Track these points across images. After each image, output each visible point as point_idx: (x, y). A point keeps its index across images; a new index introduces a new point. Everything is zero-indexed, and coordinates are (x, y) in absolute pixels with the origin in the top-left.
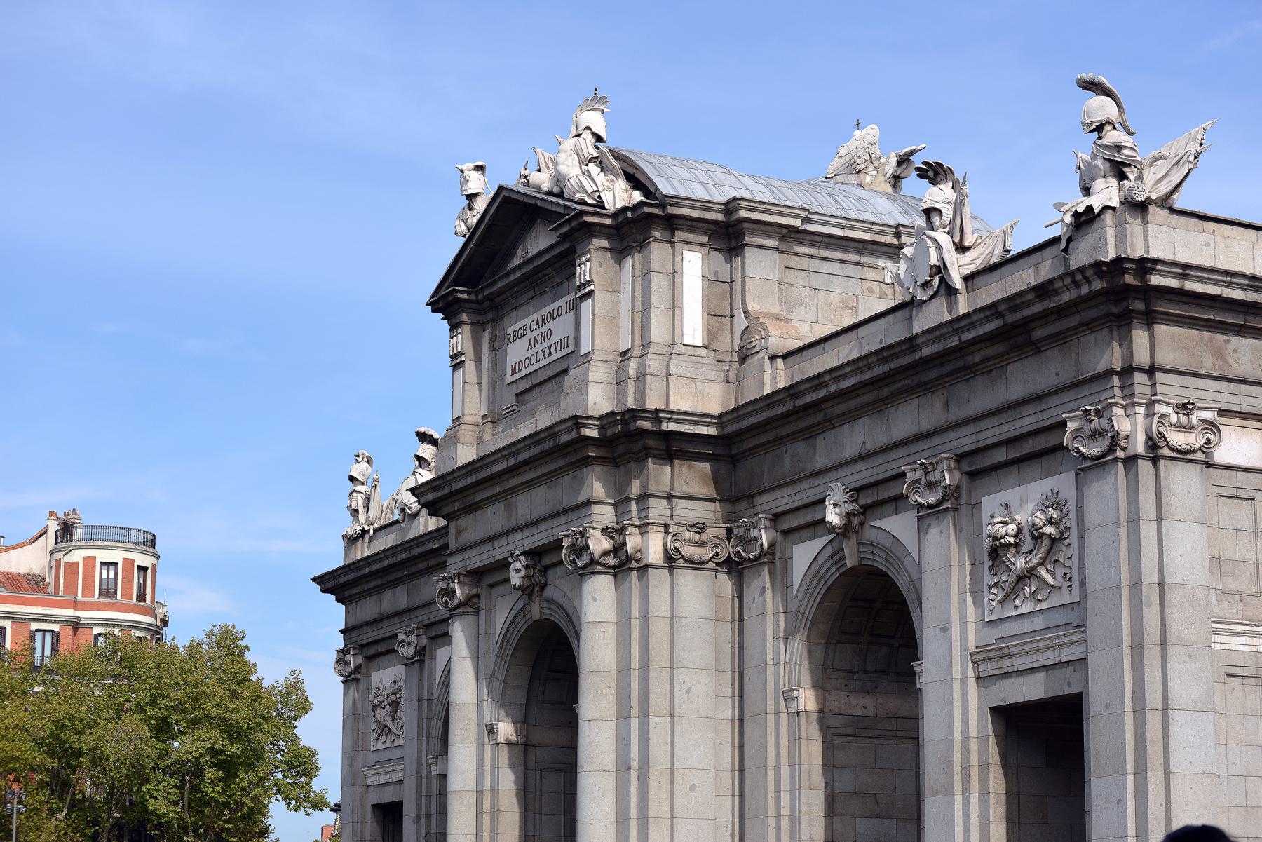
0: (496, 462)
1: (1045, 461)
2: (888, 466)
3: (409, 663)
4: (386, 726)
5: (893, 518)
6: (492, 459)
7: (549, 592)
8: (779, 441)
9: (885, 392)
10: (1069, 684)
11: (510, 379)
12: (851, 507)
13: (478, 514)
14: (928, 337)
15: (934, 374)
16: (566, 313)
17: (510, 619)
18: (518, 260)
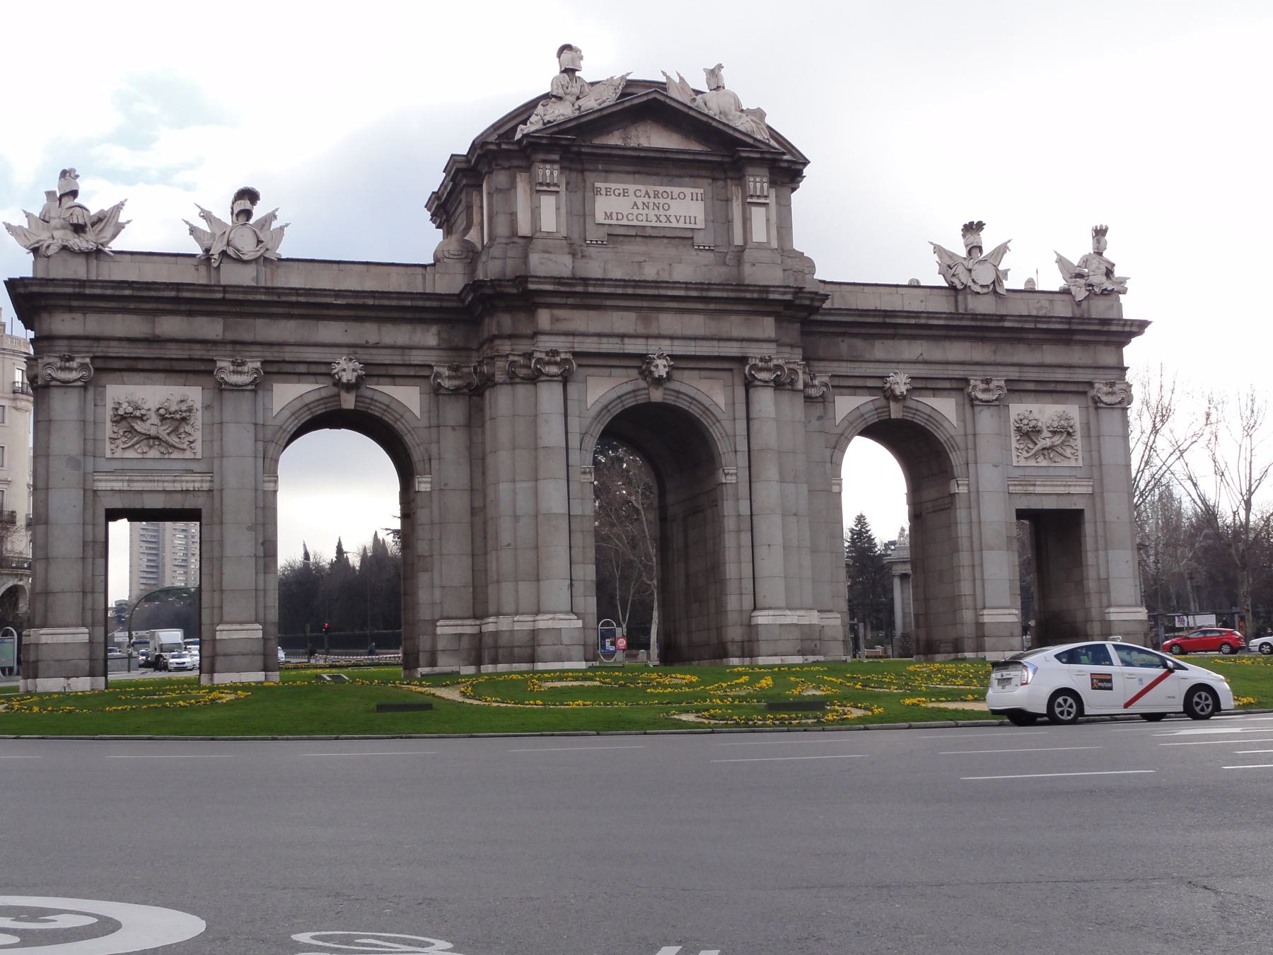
0: (673, 288)
1: (1055, 395)
2: (945, 372)
3: (222, 388)
4: (157, 438)
5: (933, 399)
6: (671, 285)
7: (674, 385)
8: (844, 334)
9: (954, 333)
10: (1075, 504)
11: (600, 218)
12: (908, 386)
13: (592, 313)
14: (1017, 318)
15: (996, 335)
16: (692, 199)
17: (615, 396)
18: (614, 139)
